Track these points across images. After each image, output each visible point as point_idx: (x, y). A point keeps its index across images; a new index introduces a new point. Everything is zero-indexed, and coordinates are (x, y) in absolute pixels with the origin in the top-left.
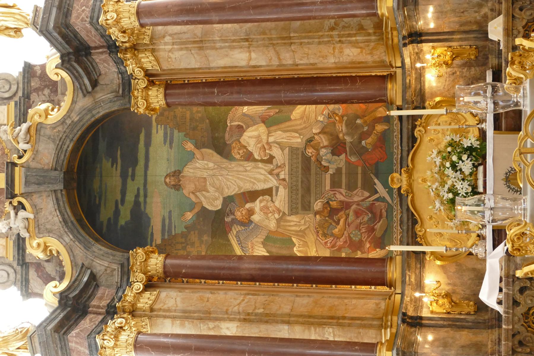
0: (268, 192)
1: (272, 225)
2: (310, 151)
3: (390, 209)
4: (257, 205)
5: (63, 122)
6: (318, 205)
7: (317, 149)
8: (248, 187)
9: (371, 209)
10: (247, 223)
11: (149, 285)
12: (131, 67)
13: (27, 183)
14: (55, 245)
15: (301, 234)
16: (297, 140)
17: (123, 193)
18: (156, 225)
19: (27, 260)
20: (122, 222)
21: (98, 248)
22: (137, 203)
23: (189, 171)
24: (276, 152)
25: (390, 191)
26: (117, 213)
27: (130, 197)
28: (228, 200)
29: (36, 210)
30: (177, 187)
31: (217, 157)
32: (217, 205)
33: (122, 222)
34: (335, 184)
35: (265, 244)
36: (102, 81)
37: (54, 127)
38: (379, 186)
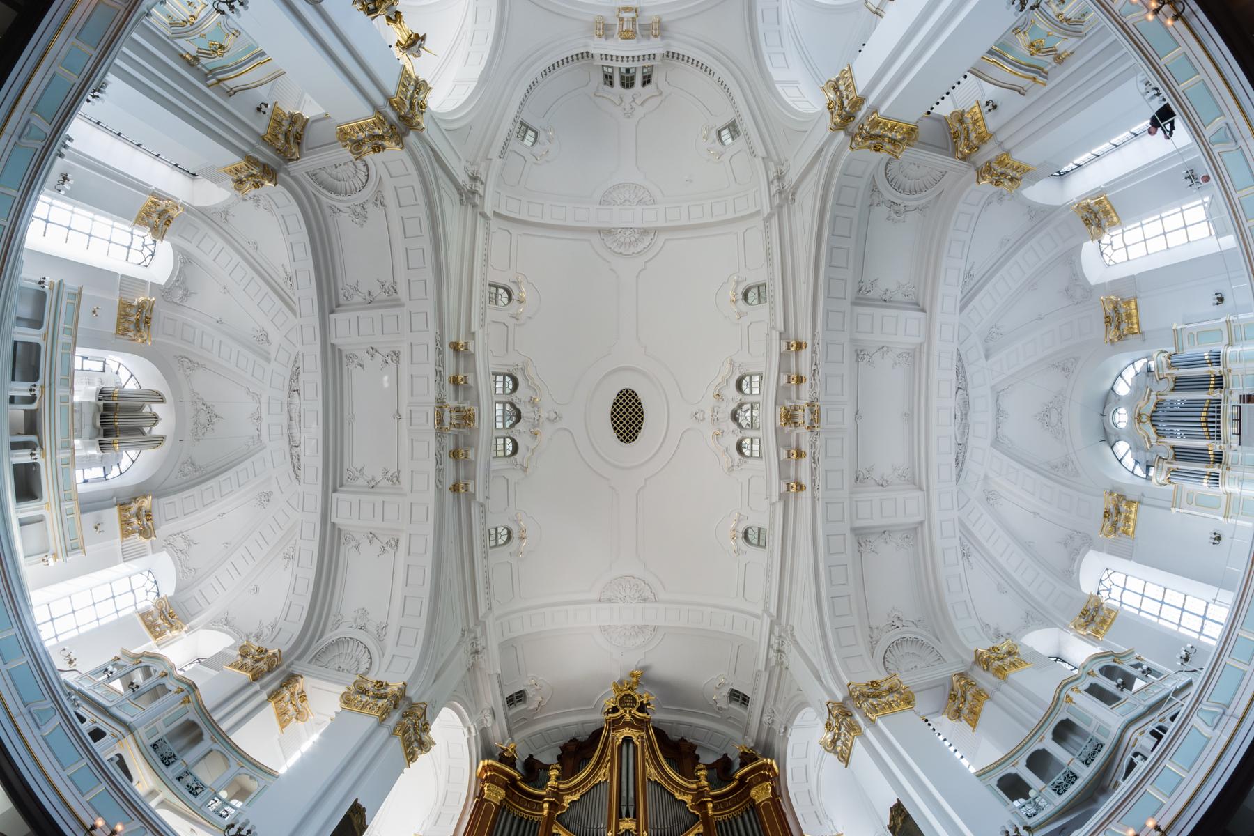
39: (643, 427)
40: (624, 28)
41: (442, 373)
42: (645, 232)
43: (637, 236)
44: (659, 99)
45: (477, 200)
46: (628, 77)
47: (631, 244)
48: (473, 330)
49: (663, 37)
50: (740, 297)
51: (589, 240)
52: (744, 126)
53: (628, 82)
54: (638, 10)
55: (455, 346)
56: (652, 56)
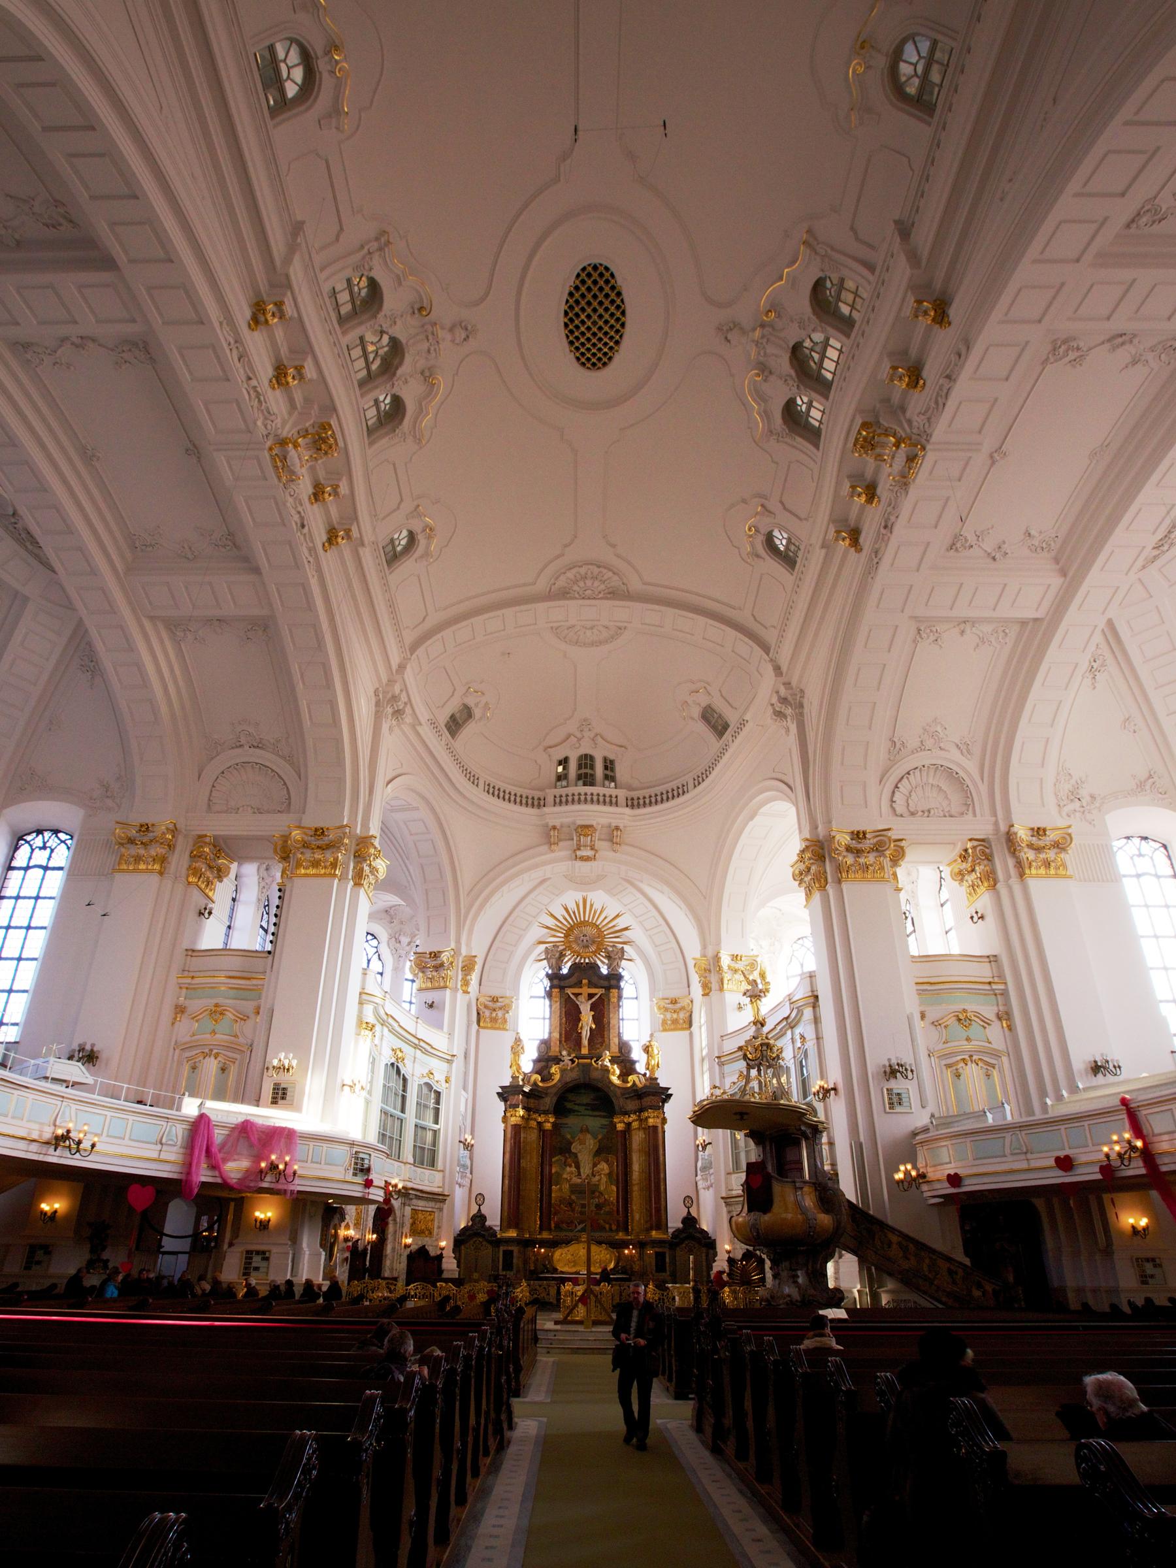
0: (579, 1174)
1: (565, 1176)
2: (597, 1194)
3: (572, 1231)
4: (573, 1169)
5: (610, 1082)
6: (573, 1197)
7: (598, 1197)
8: (582, 1165)
9: (572, 1222)
10: (566, 1164)
11: (539, 1124)
12: (633, 1117)
13: (584, 1065)
14: (557, 1077)
15: (561, 1189)
16: (602, 1188)
17: (578, 1105)
18: (564, 1121)
19: (550, 1063)
20: (566, 1104)
21: (555, 1099)
22: (574, 1111)
23: (589, 1136)
24: (597, 1178)
25: (579, 1231)
26: (570, 1101)
27: (576, 1108)
28: (576, 1155)
29: (572, 1069)
30: (581, 1131)
31: (595, 1149)
32: (573, 1150)
33: (566, 1104)
34: (583, 1206)
35: (556, 1172)
36: (629, 1101)
37: (608, 1078)
38: (582, 1226)
39: (566, 296)
40: (589, 838)
41: (883, 524)
42: (564, 594)
43: (576, 588)
44: (548, 742)
45: (783, 691)
46: (586, 767)
47: (584, 578)
48: (824, 551)
49: (546, 825)
50: (421, 539)
51: (645, 584)
52: (443, 742)
53: (586, 761)
54: (574, 857)
55: (855, 536)
56: (558, 800)
